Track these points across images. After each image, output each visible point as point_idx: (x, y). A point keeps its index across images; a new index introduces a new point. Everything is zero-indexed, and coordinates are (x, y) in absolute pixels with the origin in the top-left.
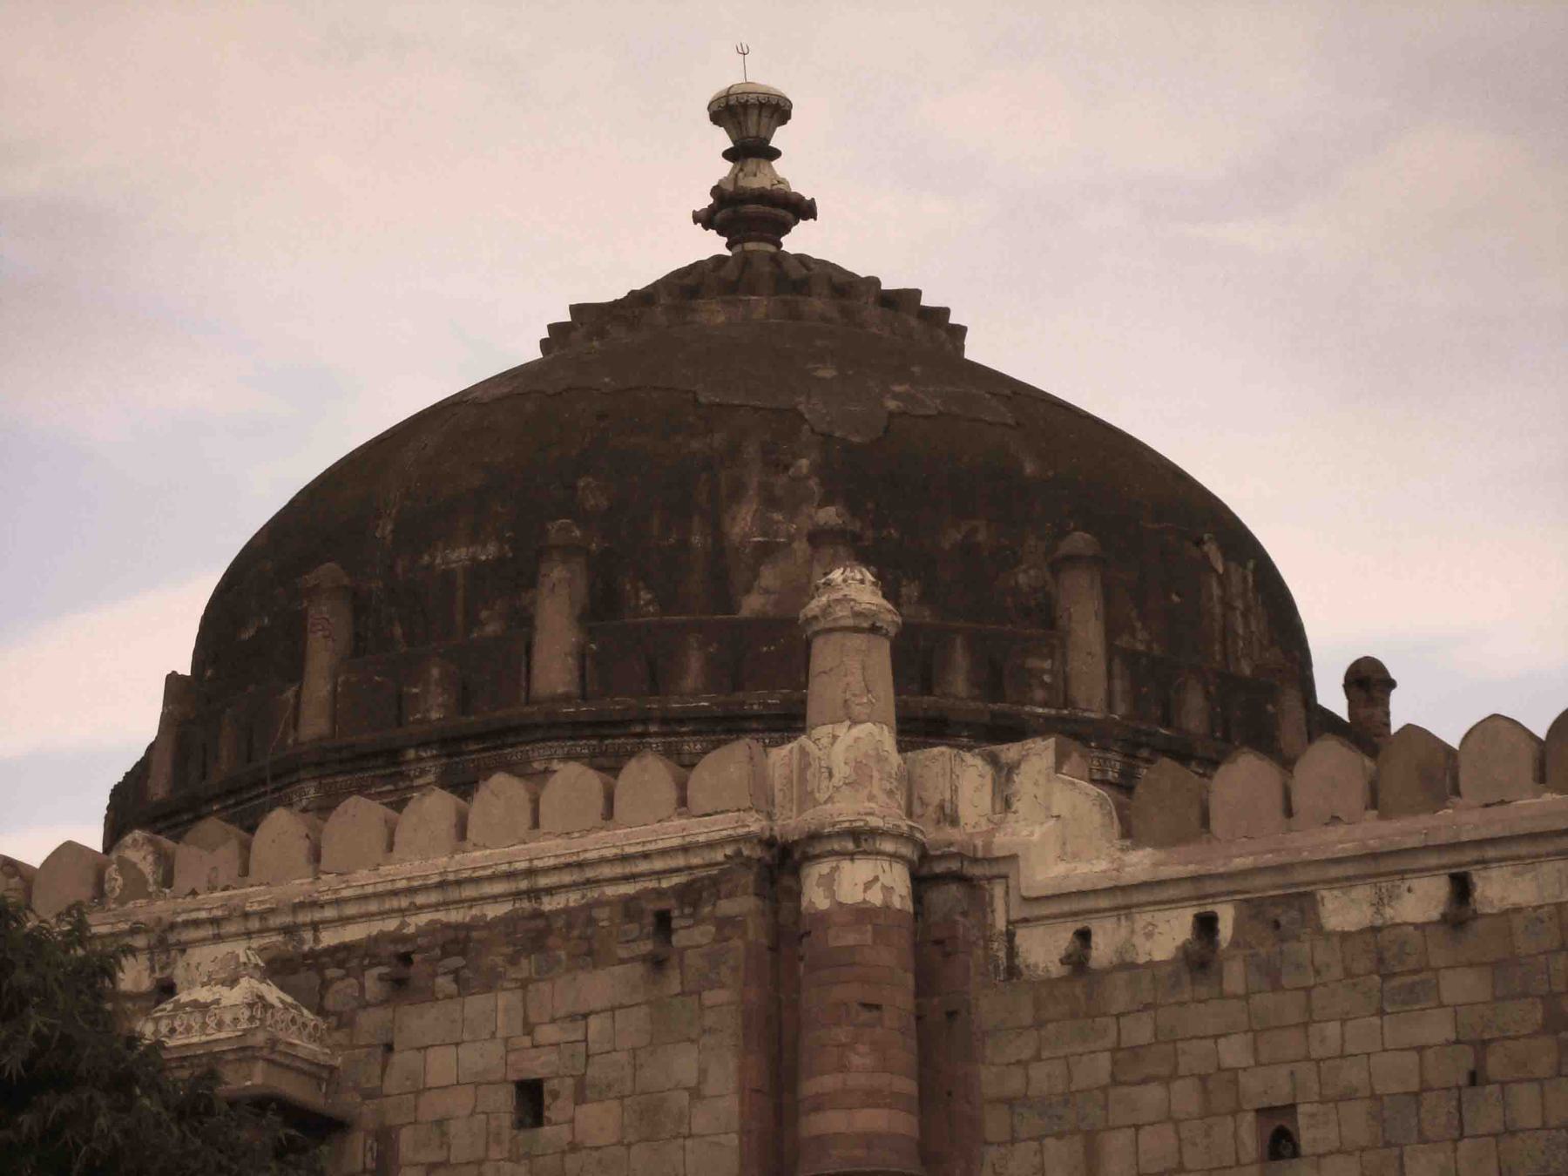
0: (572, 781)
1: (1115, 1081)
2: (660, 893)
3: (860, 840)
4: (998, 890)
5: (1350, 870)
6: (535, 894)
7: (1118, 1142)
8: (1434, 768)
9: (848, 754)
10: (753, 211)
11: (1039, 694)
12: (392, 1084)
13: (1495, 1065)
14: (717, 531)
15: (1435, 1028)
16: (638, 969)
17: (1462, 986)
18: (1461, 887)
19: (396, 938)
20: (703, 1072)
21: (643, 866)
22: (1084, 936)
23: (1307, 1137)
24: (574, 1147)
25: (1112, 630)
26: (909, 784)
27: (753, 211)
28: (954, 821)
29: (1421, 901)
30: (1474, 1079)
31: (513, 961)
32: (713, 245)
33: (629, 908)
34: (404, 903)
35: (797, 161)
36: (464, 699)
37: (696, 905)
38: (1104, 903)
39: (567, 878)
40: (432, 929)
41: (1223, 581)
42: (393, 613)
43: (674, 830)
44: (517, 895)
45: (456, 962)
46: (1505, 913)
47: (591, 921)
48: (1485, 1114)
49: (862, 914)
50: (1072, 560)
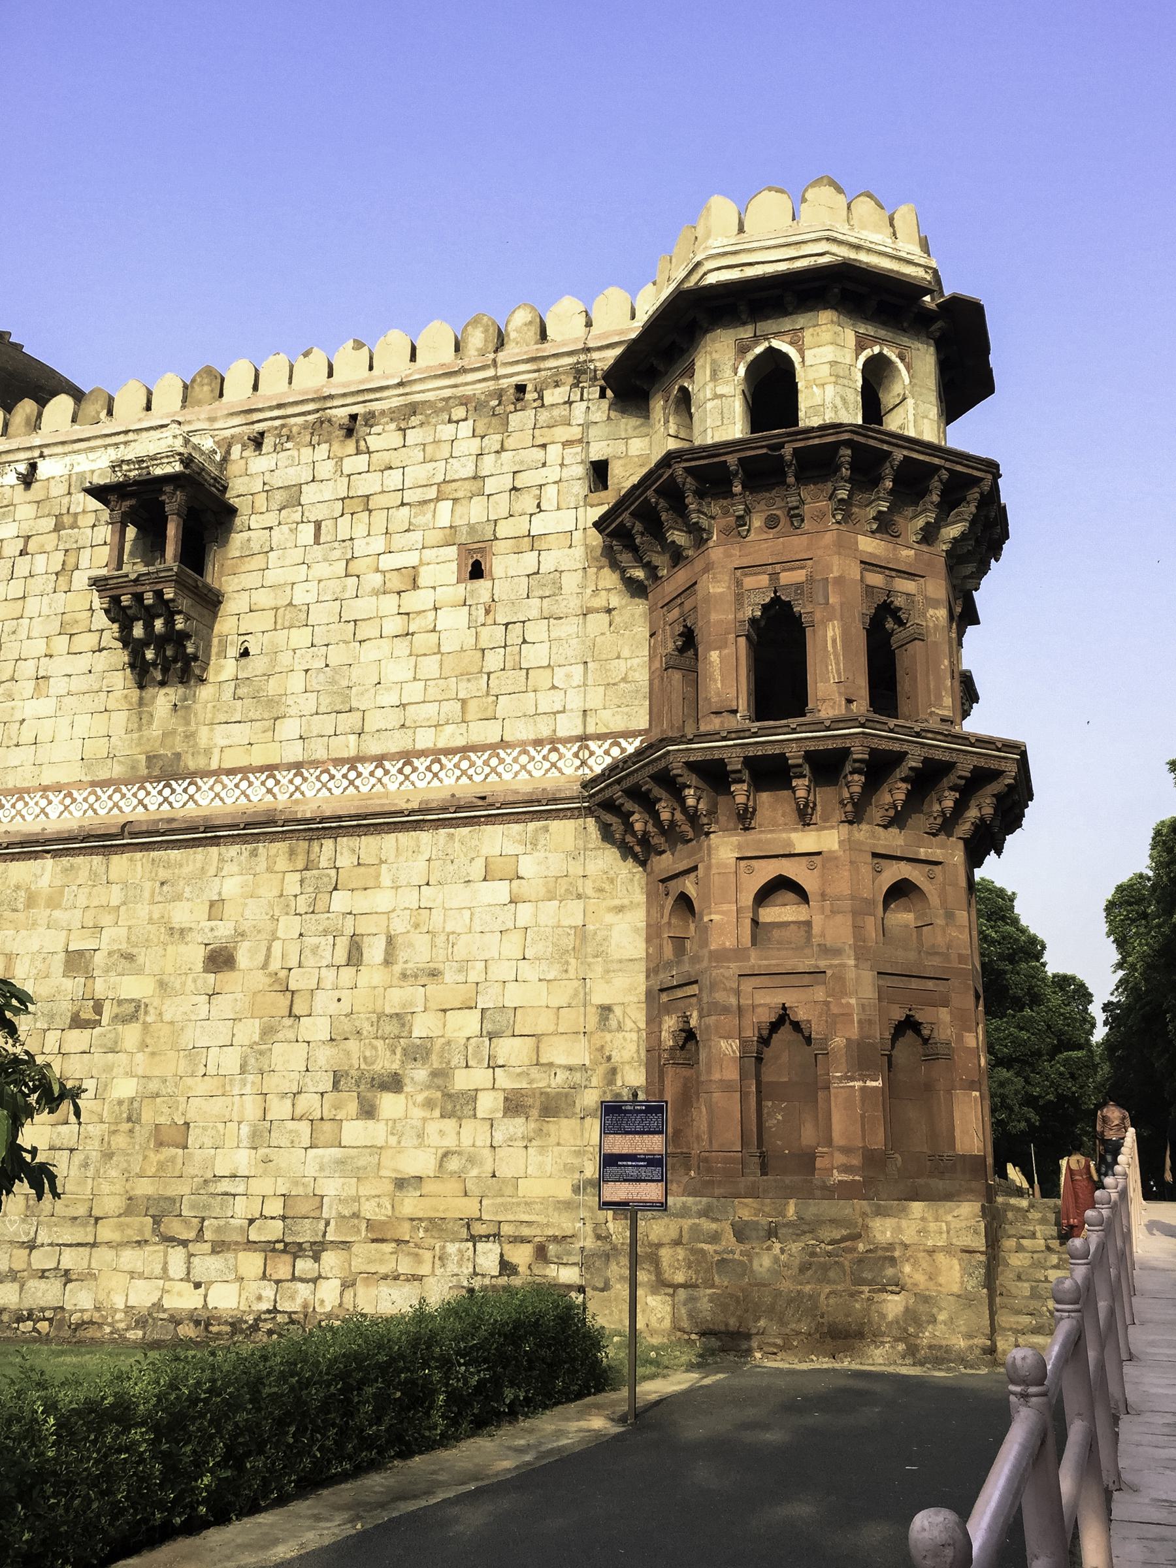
17: (25, 511)
30: (23, 553)
46: (48, 479)
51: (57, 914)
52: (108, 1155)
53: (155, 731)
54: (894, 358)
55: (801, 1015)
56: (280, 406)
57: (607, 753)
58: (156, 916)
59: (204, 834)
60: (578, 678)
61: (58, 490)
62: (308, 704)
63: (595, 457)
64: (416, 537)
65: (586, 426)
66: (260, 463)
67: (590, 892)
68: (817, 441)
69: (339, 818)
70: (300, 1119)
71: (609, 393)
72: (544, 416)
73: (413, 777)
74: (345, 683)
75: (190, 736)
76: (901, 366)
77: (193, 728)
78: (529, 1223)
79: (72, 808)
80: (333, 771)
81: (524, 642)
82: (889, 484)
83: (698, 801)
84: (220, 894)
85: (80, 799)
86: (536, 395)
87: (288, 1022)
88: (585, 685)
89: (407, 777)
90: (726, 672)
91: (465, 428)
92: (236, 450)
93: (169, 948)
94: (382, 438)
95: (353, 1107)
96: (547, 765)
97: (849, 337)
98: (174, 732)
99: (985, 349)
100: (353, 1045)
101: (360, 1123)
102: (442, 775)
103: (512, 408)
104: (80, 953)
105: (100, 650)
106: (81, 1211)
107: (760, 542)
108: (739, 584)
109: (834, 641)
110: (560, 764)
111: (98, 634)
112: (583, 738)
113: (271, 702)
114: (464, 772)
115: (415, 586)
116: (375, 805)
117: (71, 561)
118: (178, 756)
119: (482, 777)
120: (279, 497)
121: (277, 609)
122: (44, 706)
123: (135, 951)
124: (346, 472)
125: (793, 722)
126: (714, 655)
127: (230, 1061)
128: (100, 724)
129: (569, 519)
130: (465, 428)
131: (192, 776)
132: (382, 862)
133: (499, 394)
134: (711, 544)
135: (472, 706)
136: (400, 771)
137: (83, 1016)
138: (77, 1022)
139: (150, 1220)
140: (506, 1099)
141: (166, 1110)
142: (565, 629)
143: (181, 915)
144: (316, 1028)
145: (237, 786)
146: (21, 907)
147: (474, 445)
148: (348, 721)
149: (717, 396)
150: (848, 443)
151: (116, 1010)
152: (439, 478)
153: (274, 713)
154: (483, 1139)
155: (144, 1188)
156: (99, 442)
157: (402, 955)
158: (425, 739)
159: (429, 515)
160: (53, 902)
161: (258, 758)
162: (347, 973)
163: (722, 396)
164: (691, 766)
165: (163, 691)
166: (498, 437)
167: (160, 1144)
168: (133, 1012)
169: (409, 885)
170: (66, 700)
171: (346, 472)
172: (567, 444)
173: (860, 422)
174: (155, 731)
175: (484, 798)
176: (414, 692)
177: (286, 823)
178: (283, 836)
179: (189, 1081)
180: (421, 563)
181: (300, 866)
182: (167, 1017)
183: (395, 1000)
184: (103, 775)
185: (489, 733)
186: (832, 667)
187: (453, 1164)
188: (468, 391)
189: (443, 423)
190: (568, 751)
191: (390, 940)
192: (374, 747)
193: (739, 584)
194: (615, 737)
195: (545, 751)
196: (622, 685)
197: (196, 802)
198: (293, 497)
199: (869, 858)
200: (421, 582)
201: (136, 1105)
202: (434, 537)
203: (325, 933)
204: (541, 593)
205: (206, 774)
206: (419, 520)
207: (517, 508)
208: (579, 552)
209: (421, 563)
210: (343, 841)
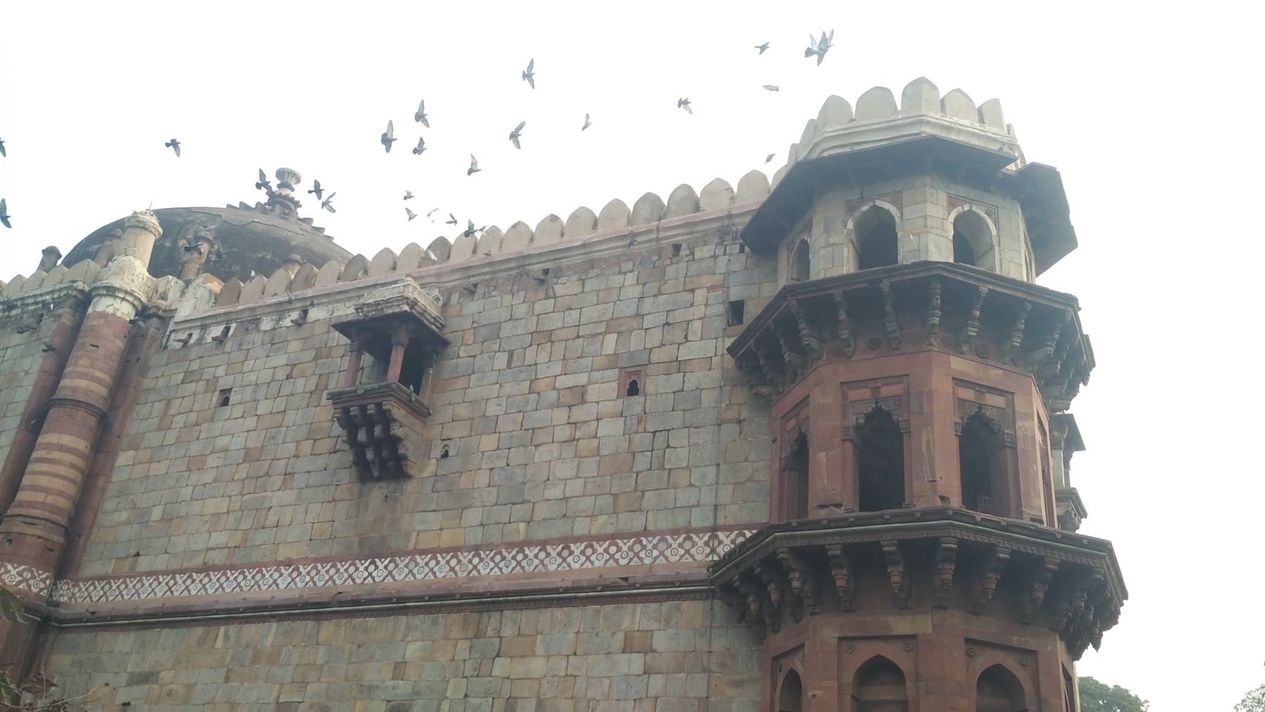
7: (176, 403)
15: (281, 360)
17: (294, 346)
23: (233, 398)
30: (288, 377)
49: (103, 315)
51: (275, 669)
54: (983, 214)
59: (395, 605)
60: (711, 478)
61: (320, 330)
62: (492, 496)
63: (733, 299)
64: (586, 362)
65: (727, 274)
66: (472, 307)
67: (714, 667)
68: (910, 277)
69: (506, 593)
71: (747, 249)
72: (694, 267)
73: (570, 560)
74: (520, 479)
76: (989, 221)
80: (505, 553)
81: (668, 446)
83: (803, 583)
84: (404, 656)
86: (688, 252)
88: (717, 483)
89: (564, 560)
91: (630, 279)
92: (455, 298)
93: (359, 703)
94: (565, 287)
97: (943, 198)
99: (1064, 209)
103: (668, 262)
104: (288, 704)
109: (928, 446)
110: (693, 551)
112: (714, 529)
114: (612, 556)
115: (583, 401)
116: (536, 583)
118: (384, 538)
119: (626, 561)
120: (483, 332)
121: (473, 419)
122: (288, 496)
124: (536, 312)
125: (887, 513)
126: (822, 456)
129: (707, 348)
130: (630, 279)
131: (392, 554)
132: (538, 633)
133: (660, 252)
134: (821, 363)
136: (559, 554)
143: (371, 674)
145: (427, 564)
146: (247, 662)
152: (608, 316)
153: (461, 501)
156: (354, 294)
158: (581, 527)
159: (598, 346)
160: (273, 660)
161: (447, 539)
164: (795, 551)
166: (657, 284)
169: (559, 654)
170: (305, 492)
171: (536, 312)
172: (710, 289)
173: (951, 260)
175: (626, 579)
176: (575, 487)
177: (463, 596)
180: (589, 383)
181: (471, 633)
184: (324, 552)
185: (637, 523)
189: (614, 274)
190: (701, 540)
192: (541, 534)
193: (844, 395)
194: (740, 528)
195: (681, 540)
196: (749, 484)
197: (393, 577)
199: (962, 644)
202: (599, 361)
203: (486, 694)
208: (716, 374)
210: (507, 614)
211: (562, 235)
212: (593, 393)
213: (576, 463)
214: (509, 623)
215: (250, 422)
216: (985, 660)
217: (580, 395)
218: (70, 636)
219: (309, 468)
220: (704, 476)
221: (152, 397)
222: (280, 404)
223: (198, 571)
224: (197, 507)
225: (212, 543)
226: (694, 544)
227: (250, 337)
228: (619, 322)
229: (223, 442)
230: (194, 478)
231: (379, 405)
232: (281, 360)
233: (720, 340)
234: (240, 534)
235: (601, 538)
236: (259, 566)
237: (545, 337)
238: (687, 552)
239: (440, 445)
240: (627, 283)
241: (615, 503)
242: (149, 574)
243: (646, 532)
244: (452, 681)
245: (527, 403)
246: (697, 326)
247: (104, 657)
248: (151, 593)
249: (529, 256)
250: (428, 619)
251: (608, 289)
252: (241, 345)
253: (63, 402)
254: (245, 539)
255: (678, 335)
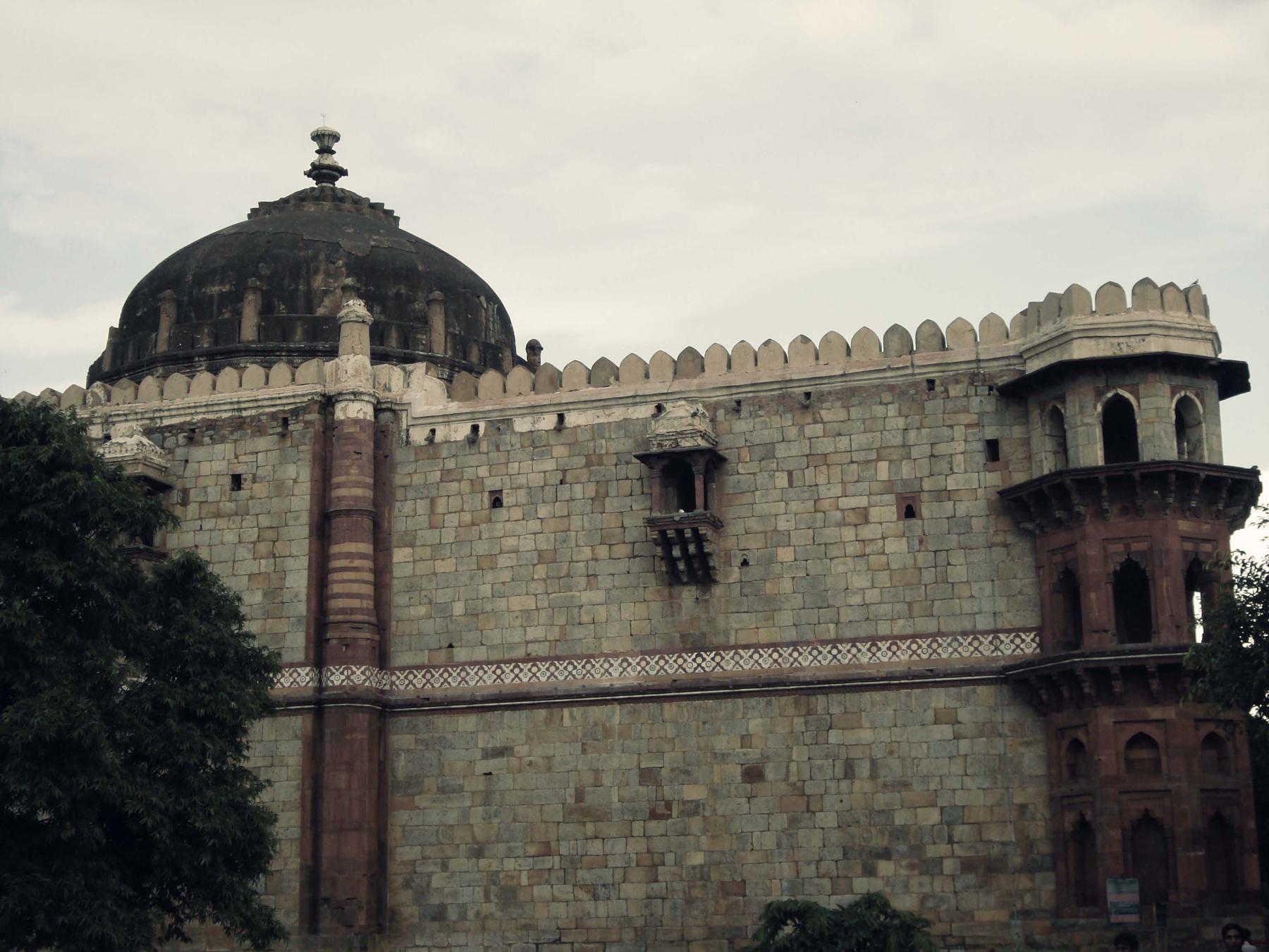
0: (254, 371)
1: (442, 481)
2: (284, 411)
3: (356, 395)
4: (404, 414)
5: (525, 411)
6: (240, 410)
8: (556, 379)
9: (352, 366)
10: (325, 173)
11: (421, 347)
12: (188, 473)
13: (569, 478)
14: (308, 284)
15: (549, 465)
16: (276, 438)
17: (559, 451)
18: (561, 418)
19: (189, 423)
20: (298, 474)
21: (279, 402)
22: (433, 431)
23: (505, 501)
24: (252, 498)
25: (447, 325)
26: (375, 376)
27: (325, 173)
28: (390, 390)
29: (549, 422)
30: (562, 482)
31: (232, 433)
32: (311, 183)
33: (273, 416)
34: (193, 411)
35: (340, 158)
36: (216, 340)
37: (297, 416)
38: (440, 420)
39: (251, 405)
40: (203, 420)
41: (486, 310)
42: (190, 310)
43: (290, 390)
44: (233, 410)
45: (212, 432)
47: (260, 420)
48: (565, 493)
49: (356, 421)
50: (435, 301)
52: (690, 901)
53: (684, 617)
55: (1158, 814)
56: (753, 385)
57: (1012, 641)
58: (702, 745)
59: (733, 689)
60: (988, 591)
62: (797, 601)
64: (864, 486)
65: (981, 414)
66: (741, 426)
67: (1007, 732)
70: (823, 877)
72: (950, 405)
73: (879, 654)
75: (710, 621)
77: (712, 614)
78: (983, 937)
79: (629, 669)
81: (949, 564)
82: (1197, 491)
85: (634, 663)
87: (807, 815)
89: (874, 654)
90: (1099, 605)
91: (892, 410)
92: (721, 413)
94: (832, 413)
95: (859, 869)
96: (972, 649)
97: (1166, 389)
98: (699, 617)
100: (853, 830)
101: (864, 880)
102: (899, 653)
103: (925, 397)
104: (650, 770)
105: (635, 557)
106: (675, 936)
107: (1118, 524)
108: (1105, 549)
111: (630, 546)
112: (995, 632)
113: (769, 599)
114: (914, 652)
115: (867, 521)
117: (602, 491)
118: (704, 635)
122: (599, 596)
123: (689, 768)
126: (1093, 595)
127: (769, 841)
128: (641, 610)
130: (892, 410)
131: (718, 649)
132: (861, 711)
133: (915, 385)
135: (916, 607)
136: (869, 650)
137: (658, 811)
138: (654, 815)
139: (726, 942)
140: (962, 863)
141: (727, 872)
142: (977, 556)
143: (721, 744)
144: (828, 819)
145: (751, 657)
147: (901, 423)
148: (827, 614)
149: (1084, 424)
150: (1176, 472)
151: (681, 807)
152: (877, 445)
153: (771, 606)
154: (949, 887)
155: (719, 921)
157: (882, 772)
158: (884, 629)
161: (764, 637)
162: (844, 785)
163: (1087, 425)
164: (1086, 670)
165: (686, 589)
167: (726, 894)
168: (693, 809)
172: (968, 426)
174: (684, 617)
178: (790, 692)
179: (742, 854)
180: (870, 505)
181: (803, 711)
182: (720, 812)
183: (882, 800)
185: (932, 626)
186: (1167, 606)
187: (930, 903)
188: (892, 382)
191: (873, 763)
192: (849, 633)
193: (1105, 549)
195: (970, 640)
198: (768, 452)
200: (871, 519)
201: (706, 869)
202: (876, 487)
203: (827, 757)
204: (956, 530)
205: (727, 648)
206: (865, 474)
207: (936, 469)
208: (982, 503)
209: (870, 505)
211: (817, 358)
212: (875, 514)
213: (870, 576)
214: (834, 705)
215: (534, 525)
216: (1206, 729)
217: (863, 516)
218: (405, 719)
219: (612, 571)
220: (981, 589)
221: (411, 494)
222: (561, 509)
223: (525, 661)
224: (501, 604)
225: (530, 636)
226: (981, 643)
227: (507, 438)
228: (887, 451)
229: (511, 542)
230: (489, 576)
231: (695, 531)
232: (549, 465)
233: (982, 474)
234: (556, 631)
235: (903, 638)
236: (589, 657)
237: (816, 459)
238: (976, 649)
239: (739, 554)
240: (891, 413)
241: (910, 610)
242: (473, 664)
243: (940, 634)
244: (795, 748)
245: (815, 521)
246: (959, 459)
247: (449, 737)
248: (483, 681)
249: (791, 381)
250: (763, 701)
251: (874, 418)
252: (498, 449)
253: (339, 513)
254: (563, 633)
255: (944, 466)
